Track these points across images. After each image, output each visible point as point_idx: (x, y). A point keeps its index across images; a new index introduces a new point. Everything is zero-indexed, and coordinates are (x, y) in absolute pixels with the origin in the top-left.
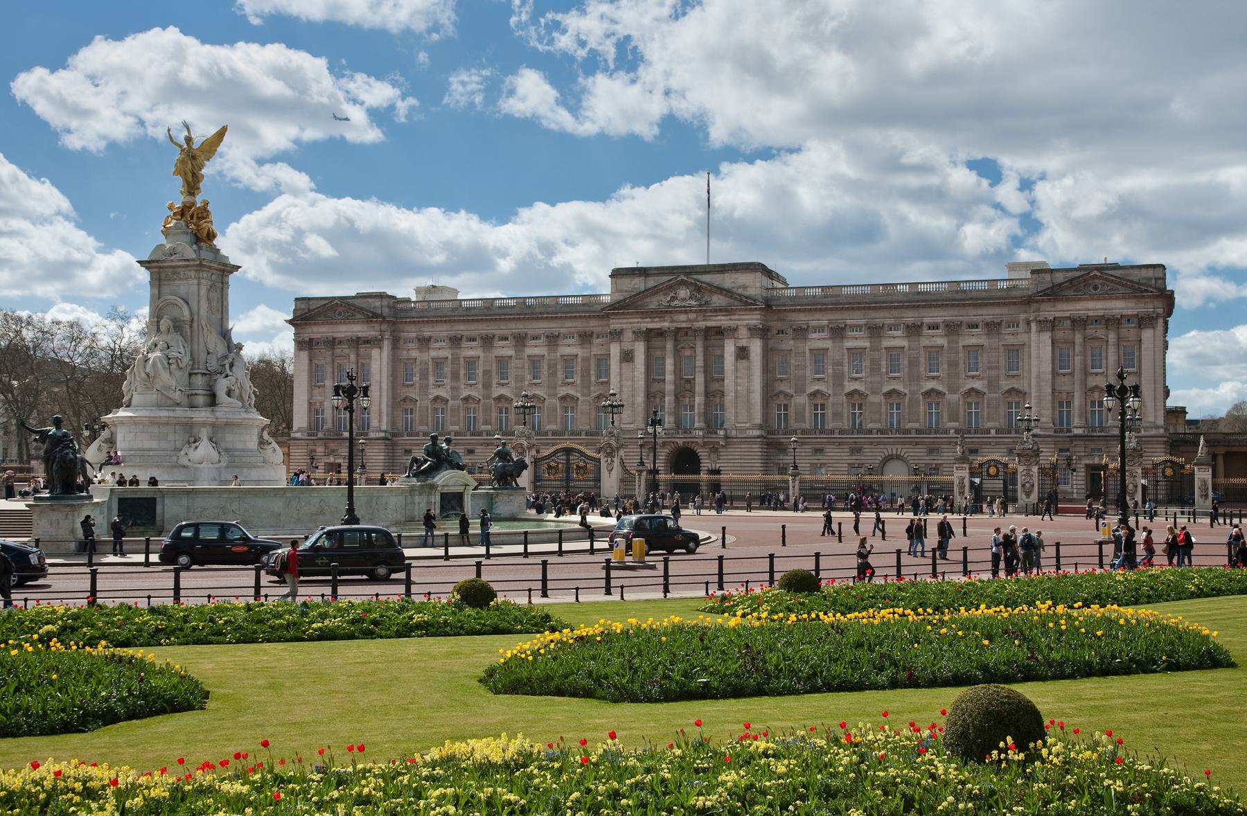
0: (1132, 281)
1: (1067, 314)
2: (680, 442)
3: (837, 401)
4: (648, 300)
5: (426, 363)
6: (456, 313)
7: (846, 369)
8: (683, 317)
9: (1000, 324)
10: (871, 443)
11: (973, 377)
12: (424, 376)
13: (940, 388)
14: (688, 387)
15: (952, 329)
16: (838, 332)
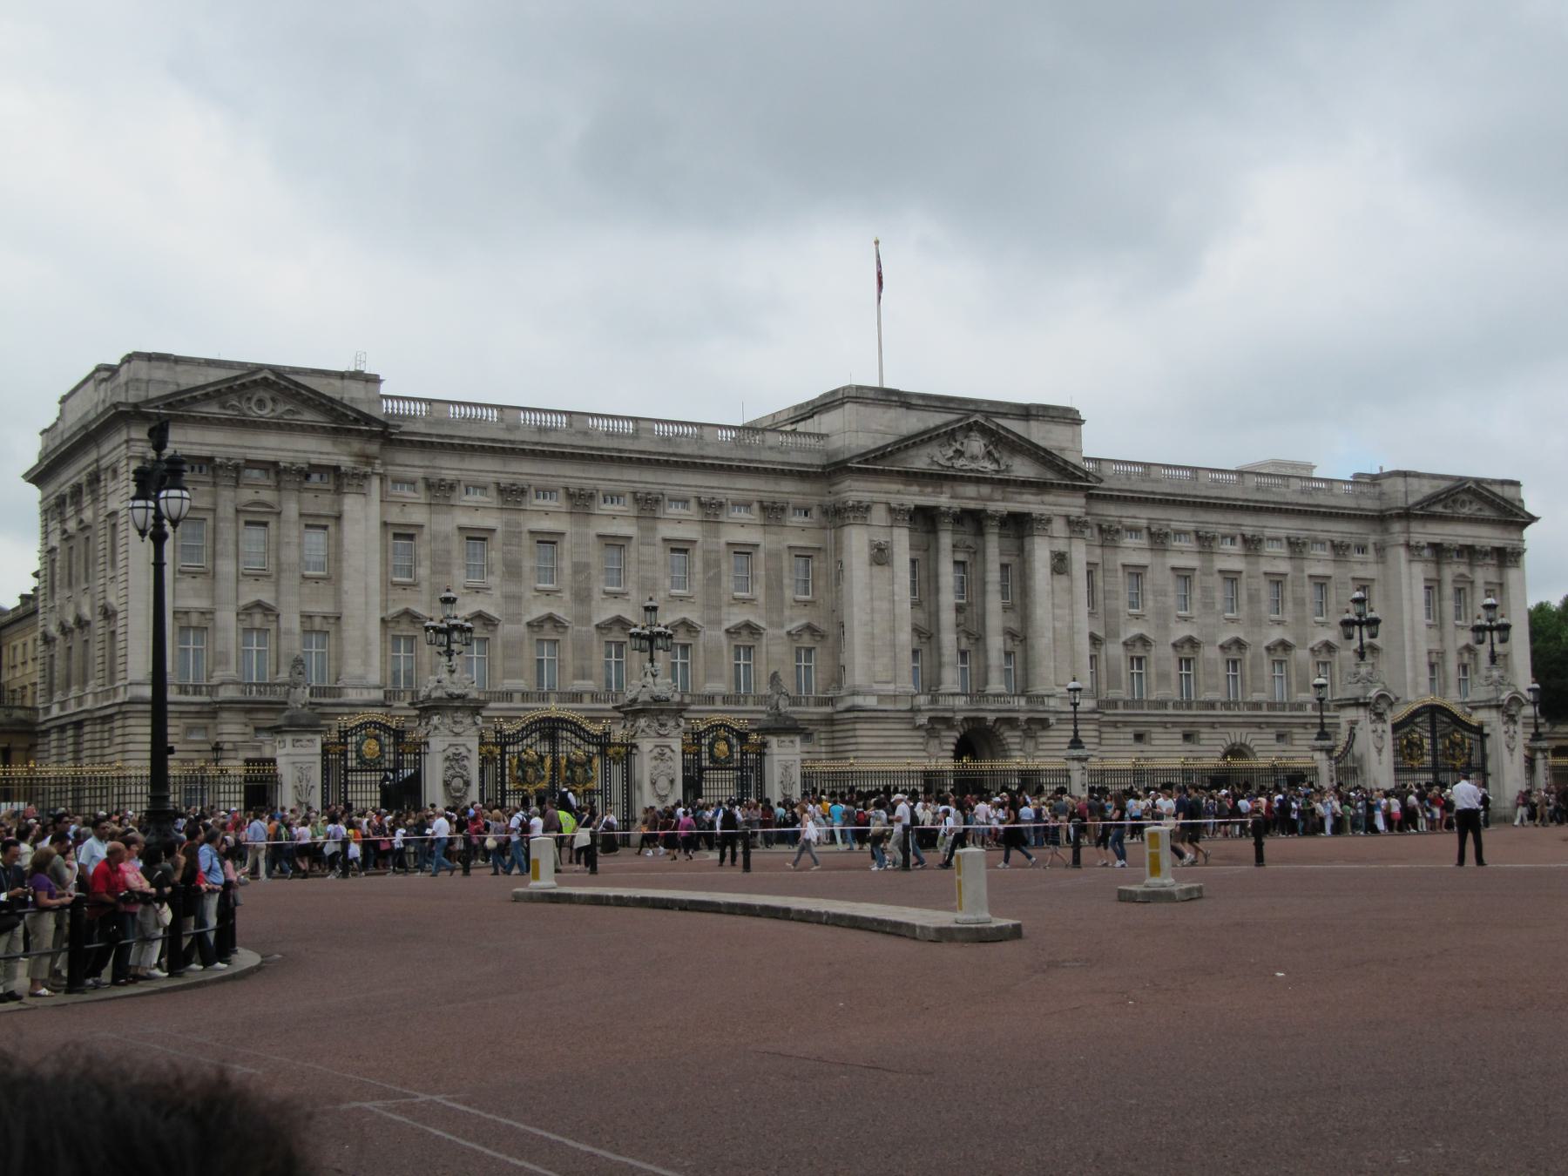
0: (1502, 498)
1: (1437, 540)
2: (991, 717)
3: (1163, 657)
4: (912, 452)
5: (447, 538)
6: (517, 436)
7: (1172, 601)
8: (970, 490)
9: (1348, 547)
10: (1212, 725)
11: (1323, 624)
12: (441, 565)
13: (1289, 639)
14: (962, 618)
15: (1296, 547)
16: (1159, 539)
